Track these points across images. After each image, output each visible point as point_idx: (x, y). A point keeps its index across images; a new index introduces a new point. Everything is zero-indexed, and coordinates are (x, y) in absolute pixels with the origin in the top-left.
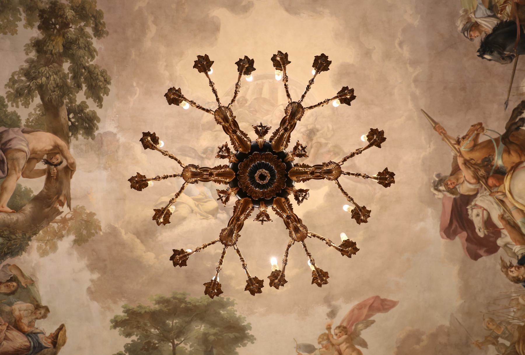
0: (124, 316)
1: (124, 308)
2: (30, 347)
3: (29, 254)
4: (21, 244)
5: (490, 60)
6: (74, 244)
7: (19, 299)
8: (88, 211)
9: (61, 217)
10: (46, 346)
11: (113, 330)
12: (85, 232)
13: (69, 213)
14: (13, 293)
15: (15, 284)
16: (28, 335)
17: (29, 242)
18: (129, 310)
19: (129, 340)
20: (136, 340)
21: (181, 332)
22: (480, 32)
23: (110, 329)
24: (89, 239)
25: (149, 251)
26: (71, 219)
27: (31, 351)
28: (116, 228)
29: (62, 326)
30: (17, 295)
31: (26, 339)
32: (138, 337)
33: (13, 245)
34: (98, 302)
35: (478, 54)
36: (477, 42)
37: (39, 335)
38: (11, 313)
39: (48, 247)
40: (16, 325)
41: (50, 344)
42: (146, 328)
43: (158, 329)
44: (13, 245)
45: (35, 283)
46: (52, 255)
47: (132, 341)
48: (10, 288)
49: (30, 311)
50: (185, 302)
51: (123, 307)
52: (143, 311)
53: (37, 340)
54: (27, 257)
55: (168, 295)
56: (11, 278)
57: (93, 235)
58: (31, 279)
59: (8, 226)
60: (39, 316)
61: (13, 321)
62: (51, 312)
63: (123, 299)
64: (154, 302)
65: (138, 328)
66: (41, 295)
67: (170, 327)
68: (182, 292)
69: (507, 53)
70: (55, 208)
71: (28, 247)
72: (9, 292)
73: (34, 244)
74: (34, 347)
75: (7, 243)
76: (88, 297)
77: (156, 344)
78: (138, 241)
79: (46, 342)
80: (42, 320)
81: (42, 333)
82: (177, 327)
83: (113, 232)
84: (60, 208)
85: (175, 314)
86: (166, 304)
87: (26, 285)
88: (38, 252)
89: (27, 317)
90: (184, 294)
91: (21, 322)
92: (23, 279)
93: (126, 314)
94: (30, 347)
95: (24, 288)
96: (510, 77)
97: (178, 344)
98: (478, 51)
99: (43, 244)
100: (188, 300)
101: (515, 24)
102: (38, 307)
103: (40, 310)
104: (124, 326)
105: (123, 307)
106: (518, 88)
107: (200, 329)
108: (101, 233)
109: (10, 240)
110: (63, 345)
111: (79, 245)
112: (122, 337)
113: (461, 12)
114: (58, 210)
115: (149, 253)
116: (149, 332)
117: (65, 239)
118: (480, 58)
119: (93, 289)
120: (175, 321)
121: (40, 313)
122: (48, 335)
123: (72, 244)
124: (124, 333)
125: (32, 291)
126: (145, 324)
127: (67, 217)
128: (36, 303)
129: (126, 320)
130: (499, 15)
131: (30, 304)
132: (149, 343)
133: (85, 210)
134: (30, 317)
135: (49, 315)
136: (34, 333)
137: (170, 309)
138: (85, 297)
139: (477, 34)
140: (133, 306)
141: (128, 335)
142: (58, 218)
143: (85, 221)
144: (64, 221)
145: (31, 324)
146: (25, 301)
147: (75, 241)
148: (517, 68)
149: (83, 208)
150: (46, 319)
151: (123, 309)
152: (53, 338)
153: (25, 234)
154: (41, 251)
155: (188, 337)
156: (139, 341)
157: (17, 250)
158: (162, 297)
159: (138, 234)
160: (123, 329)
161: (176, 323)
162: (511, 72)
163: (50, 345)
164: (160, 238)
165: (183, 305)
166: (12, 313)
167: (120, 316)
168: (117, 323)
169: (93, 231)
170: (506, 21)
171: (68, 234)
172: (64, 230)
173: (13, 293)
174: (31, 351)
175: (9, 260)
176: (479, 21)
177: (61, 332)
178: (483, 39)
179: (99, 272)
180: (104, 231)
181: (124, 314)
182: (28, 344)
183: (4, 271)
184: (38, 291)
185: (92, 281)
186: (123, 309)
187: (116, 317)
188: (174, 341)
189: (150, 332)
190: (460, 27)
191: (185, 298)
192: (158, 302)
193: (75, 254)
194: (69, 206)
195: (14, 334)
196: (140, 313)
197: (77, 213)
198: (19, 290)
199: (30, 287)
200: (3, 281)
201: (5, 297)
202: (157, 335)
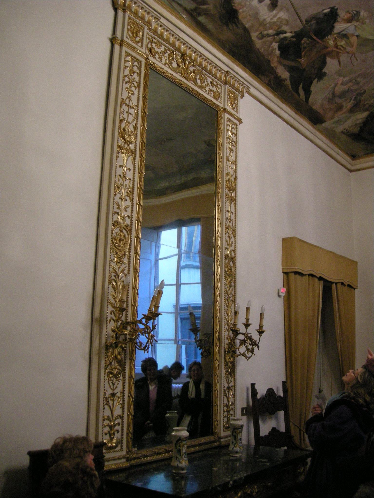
5: (323, 10)
22: (343, 20)
35: (336, 8)
36: (342, 14)
69: (313, 22)
96: (299, 12)
98: (337, 9)
101: (319, 39)
106: (288, 10)
113: (367, 21)
118: (332, 6)
130: (335, 36)
139: (346, 17)
148: (299, 21)
162: (301, 15)
170: (328, 36)
176: (349, 25)
178: (338, 17)
190: (362, 13)
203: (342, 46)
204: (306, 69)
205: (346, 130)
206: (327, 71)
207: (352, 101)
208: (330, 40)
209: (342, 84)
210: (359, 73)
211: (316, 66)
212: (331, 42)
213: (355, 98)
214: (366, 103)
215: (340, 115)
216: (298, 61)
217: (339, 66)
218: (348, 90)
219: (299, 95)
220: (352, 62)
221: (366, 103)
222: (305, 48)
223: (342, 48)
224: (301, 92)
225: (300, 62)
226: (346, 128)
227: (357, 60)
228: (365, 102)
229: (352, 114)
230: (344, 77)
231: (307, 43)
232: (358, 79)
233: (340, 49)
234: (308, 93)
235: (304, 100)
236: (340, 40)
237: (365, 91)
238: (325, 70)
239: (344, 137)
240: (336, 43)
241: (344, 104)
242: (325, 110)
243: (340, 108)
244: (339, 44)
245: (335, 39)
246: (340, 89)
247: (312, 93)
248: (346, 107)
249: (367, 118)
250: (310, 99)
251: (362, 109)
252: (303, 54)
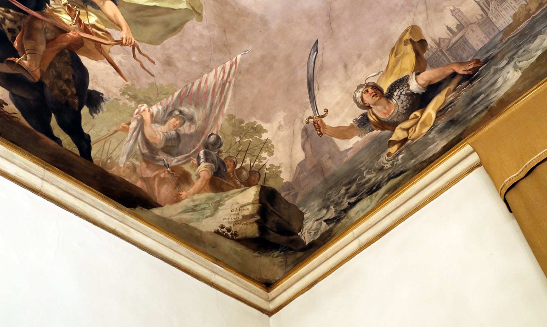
170: (49, 3)
203: (93, 26)
204: (47, 82)
205: (229, 230)
206: (98, 89)
207: (203, 165)
208: (59, 12)
209: (154, 120)
210: (176, 94)
211: (66, 76)
212: (66, 18)
213: (206, 154)
214: (238, 167)
215: (192, 195)
216: (13, 62)
217: (120, 77)
218: (178, 135)
219: (57, 140)
220: (143, 67)
221: (238, 167)
222: (10, 30)
223: (100, 33)
224: (58, 131)
225: (19, 66)
226: (227, 225)
227: (153, 62)
228: (235, 166)
229: (224, 194)
230: (150, 105)
231: (11, 20)
232: (185, 109)
233: (97, 35)
234: (83, 142)
235: (77, 152)
236: (82, 11)
237: (218, 138)
238: (91, 86)
239: (228, 245)
240: (79, 21)
241: (187, 168)
242: (145, 180)
243: (183, 179)
244: (85, 21)
245: (69, 8)
246: (158, 133)
247: (93, 139)
248: (199, 177)
249: (260, 201)
250: (94, 153)
251: (238, 183)
252: (16, 45)
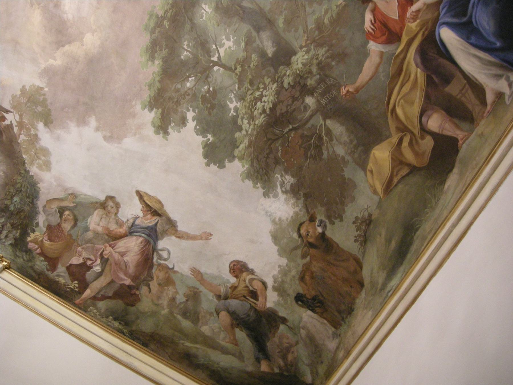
0: (156, 113)
1: (145, 107)
2: (146, 239)
3: (41, 180)
4: (29, 183)
6: (48, 127)
7: (85, 218)
8: (19, 93)
9: (16, 126)
10: (154, 223)
11: (169, 137)
12: (40, 109)
13: (14, 116)
14: (76, 220)
15: (67, 213)
16: (130, 233)
17: (30, 174)
18: (150, 102)
19: (191, 124)
20: (194, 114)
21: (203, 45)
23: (167, 140)
24: (49, 108)
25: (82, 39)
26: (21, 116)
27: (152, 241)
28: (45, 68)
29: (138, 193)
30: (80, 218)
31: (135, 238)
32: (191, 109)
33: (26, 192)
34: (126, 136)
37: (137, 222)
38: (97, 234)
39: (43, 158)
40: (114, 238)
41: (155, 218)
42: (182, 92)
43: (189, 76)
44: (27, 192)
45: (75, 192)
46: (53, 159)
47: (193, 120)
48: (69, 219)
49: (104, 216)
50: (163, 18)
51: (144, 108)
52: (158, 85)
53: (142, 228)
54: (45, 185)
55: (145, 39)
56: (59, 212)
57: (45, 100)
58: (69, 194)
59: (6, 184)
60: (114, 210)
61: (106, 237)
62: (116, 196)
63: (134, 103)
64: (150, 63)
65: (178, 103)
66: (91, 195)
67: (191, 56)
68: (147, 17)
70: (5, 127)
71: (35, 178)
72: (72, 223)
73: (34, 170)
74: (149, 235)
75: (22, 195)
76: (116, 145)
77: (209, 89)
78: (67, 47)
79: (150, 221)
80: (120, 210)
81: (137, 218)
82: (194, 46)
83: (48, 73)
84: (7, 122)
85: (175, 41)
86: (158, 47)
87: (73, 203)
88: (43, 171)
89: (109, 222)
90: (151, 16)
91: (112, 231)
92: (66, 202)
93: (155, 109)
94: (146, 239)
95: (76, 207)
97: (219, 58)
99: (37, 161)
100: (161, 13)
102: (103, 205)
103: (108, 205)
104: (170, 121)
105: (144, 108)
107: (206, 12)
108: (46, 89)
109: (21, 191)
110: (163, 206)
111: (52, 123)
112: (184, 130)
114: (8, 125)
115: (84, 40)
116: (189, 91)
117: (40, 135)
119: (108, 134)
120: (185, 47)
121: (112, 207)
122: (141, 214)
123: (47, 130)
124: (179, 126)
125: (82, 201)
126: (177, 91)
127: (18, 120)
128: (98, 205)
129: (162, 114)
131: (96, 212)
132: (204, 99)
133: (16, 96)
134: (111, 220)
135: (118, 199)
136: (132, 226)
137: (167, 45)
138: (113, 148)
140: (147, 95)
141: (183, 122)
142: (16, 129)
143: (28, 101)
144: (21, 125)
145: (120, 224)
146: (90, 214)
147: (46, 124)
149: (14, 97)
150: (122, 205)
151: (146, 110)
152: (148, 211)
153: (21, 173)
154: (44, 167)
155: (213, 36)
156: (197, 111)
157: (33, 191)
158: (147, 49)
159: (59, 44)
160: (173, 125)
161: (188, 46)
163: (156, 219)
164: (70, 17)
165: (166, 23)
166: (97, 234)
167: (154, 118)
168: (162, 127)
169: (41, 98)
171: (36, 129)
172: (31, 130)
173: (76, 220)
174: (152, 241)
175: (40, 203)
177: (146, 199)
179: (90, 116)
180: (45, 85)
181: (153, 112)
182: (141, 239)
183: (48, 215)
184: (86, 195)
185: (97, 129)
186: (146, 110)
187: (153, 124)
188: (213, 62)
189: (189, 89)
191: (157, 16)
192: (152, 58)
193: (59, 132)
194: (7, 111)
195: (122, 245)
196: (159, 90)
197: (17, 107)
198: (76, 212)
199: (77, 200)
200: (59, 221)
201: (76, 229)
202: (197, 81)
